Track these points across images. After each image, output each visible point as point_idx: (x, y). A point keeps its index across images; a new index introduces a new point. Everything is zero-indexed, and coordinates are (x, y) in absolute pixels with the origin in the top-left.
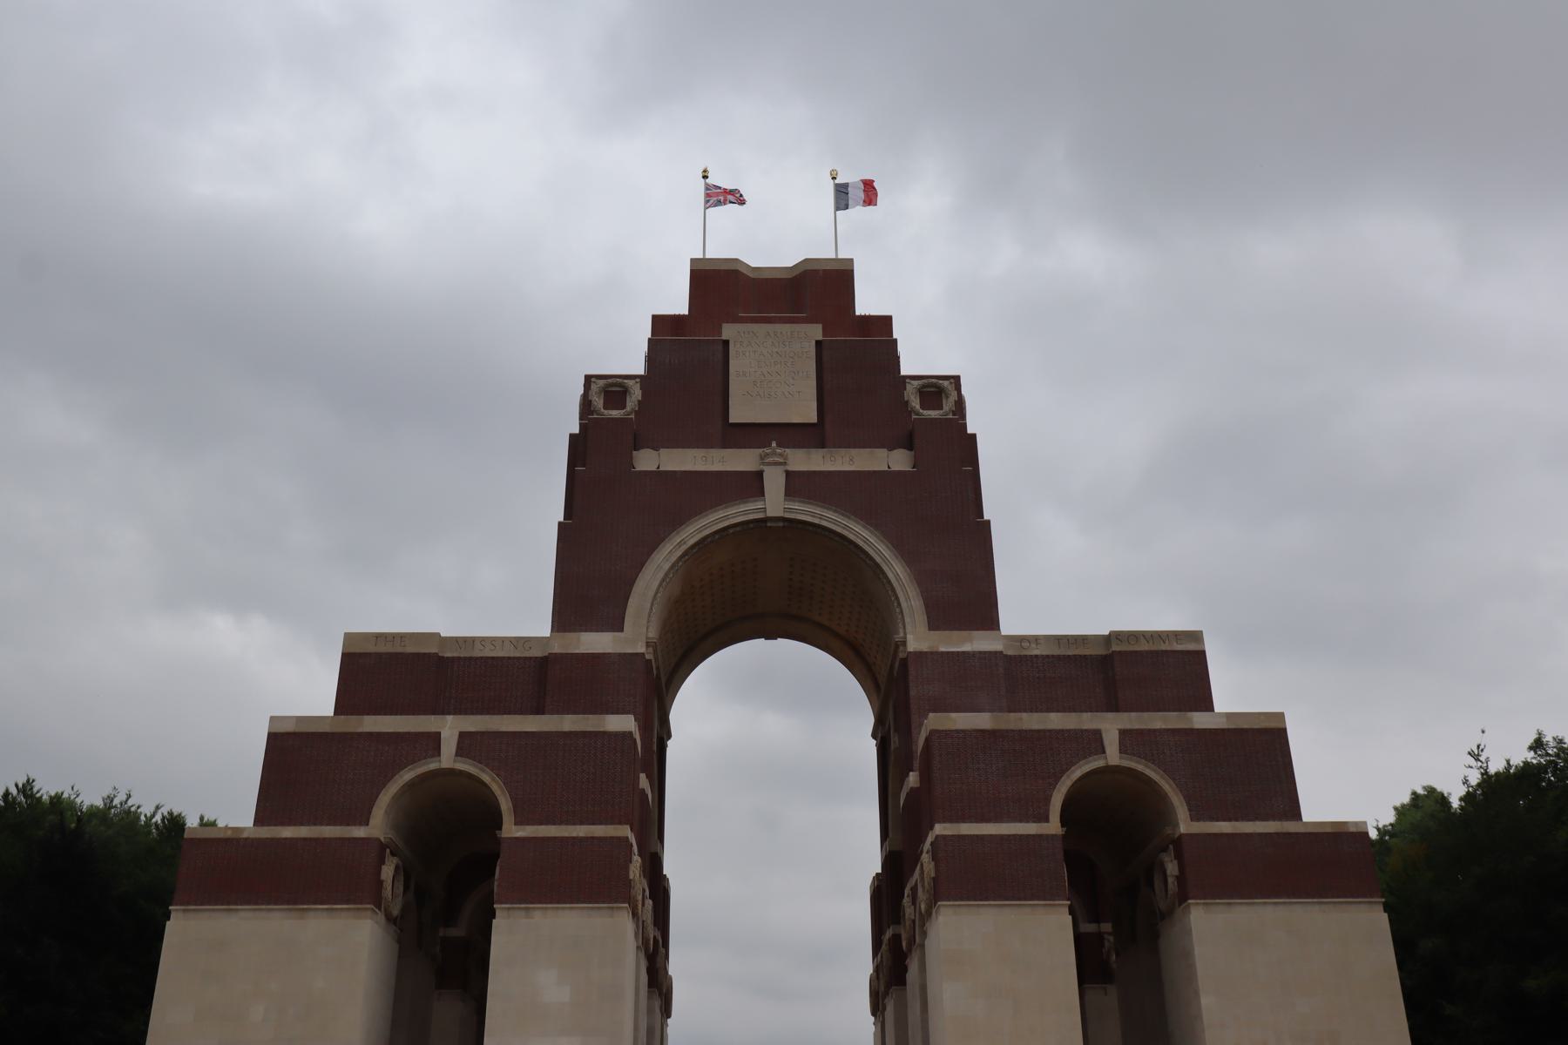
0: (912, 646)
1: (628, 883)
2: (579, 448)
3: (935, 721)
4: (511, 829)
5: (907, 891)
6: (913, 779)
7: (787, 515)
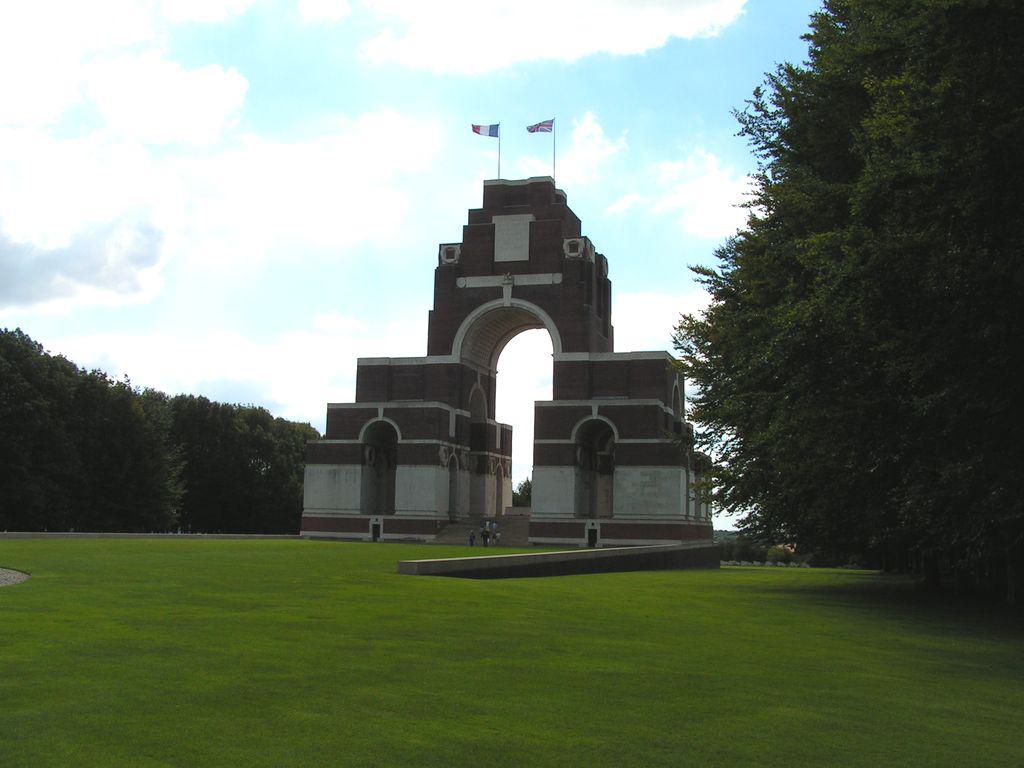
2: (439, 273)
4: (400, 441)
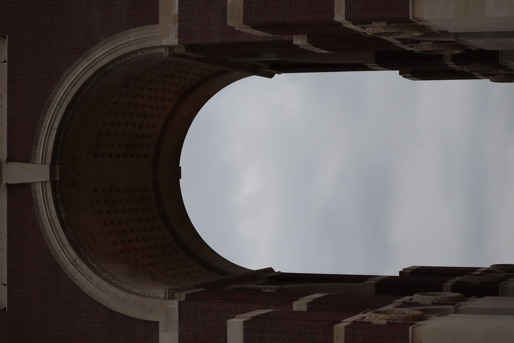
0: (173, 40)
1: (390, 325)
3: (235, 19)
5: (407, 48)
6: (300, 41)
7: (49, 161)
